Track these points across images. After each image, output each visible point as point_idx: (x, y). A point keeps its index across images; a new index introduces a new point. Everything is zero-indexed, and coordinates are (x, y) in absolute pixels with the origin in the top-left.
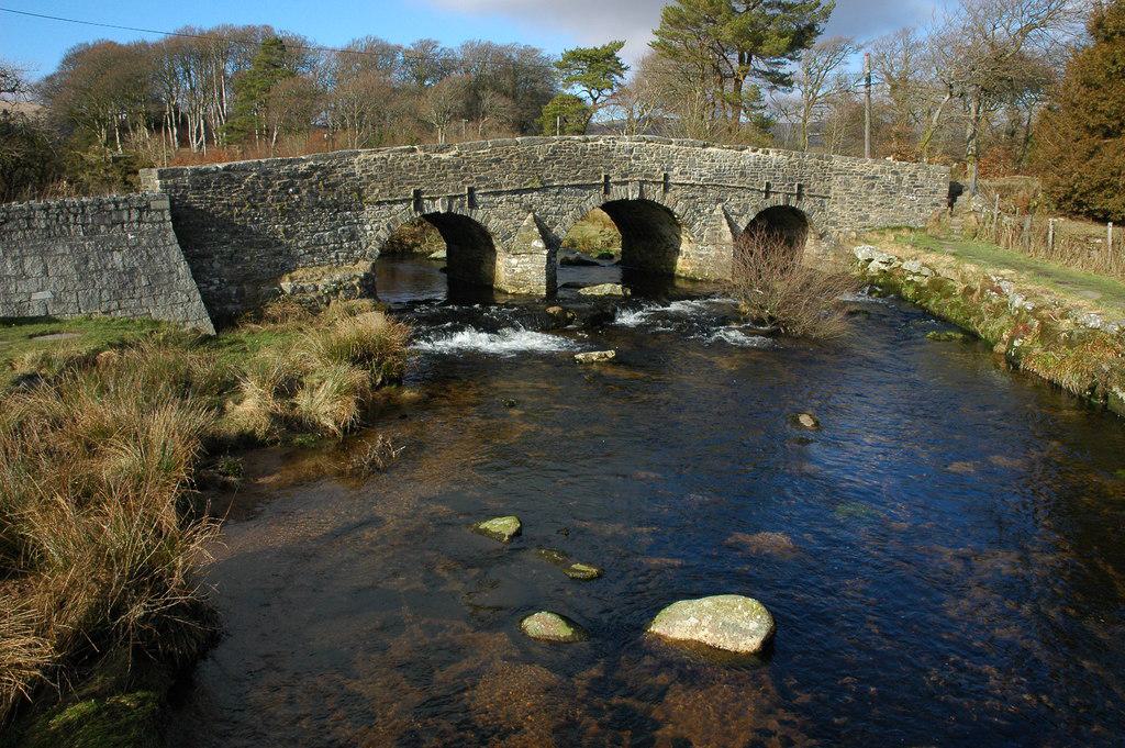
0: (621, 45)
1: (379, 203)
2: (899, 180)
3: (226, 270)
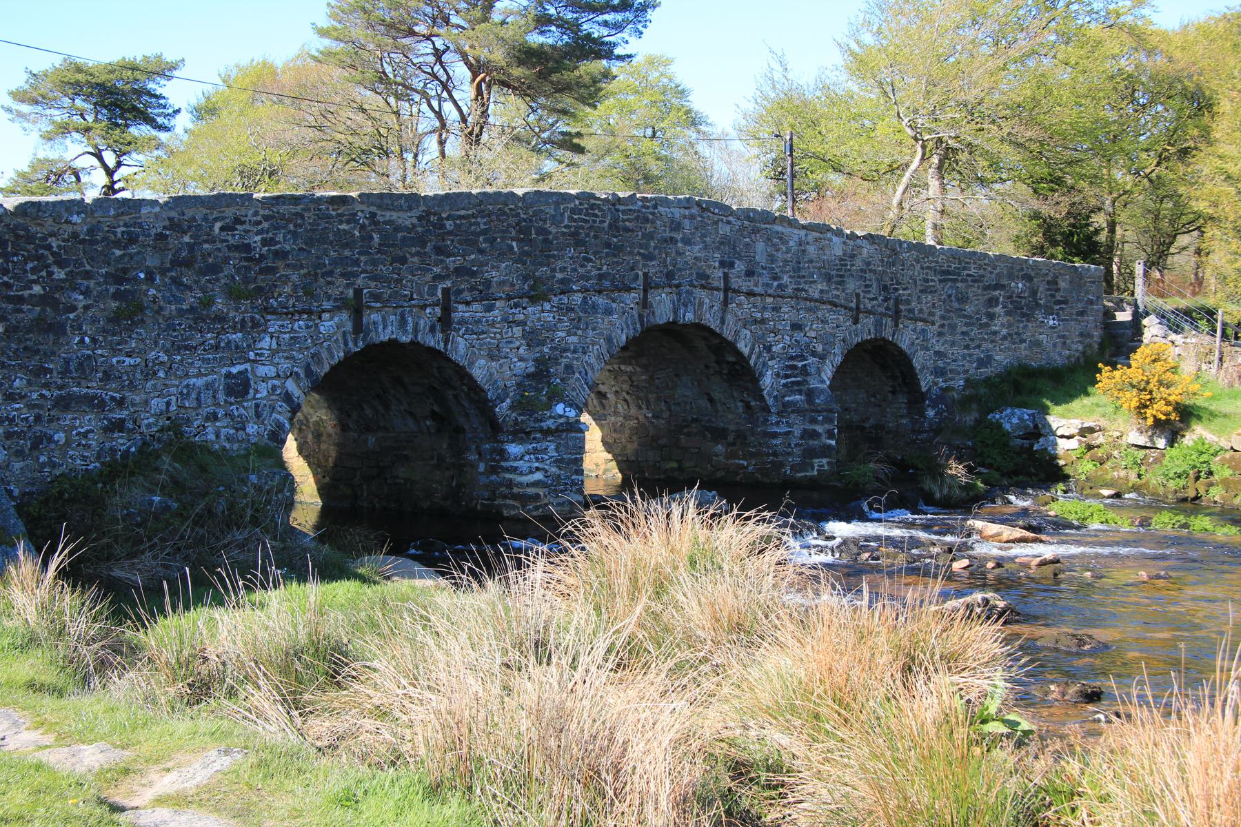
0: (164, 70)
1: (290, 314)
2: (1034, 293)
3: (18, 465)
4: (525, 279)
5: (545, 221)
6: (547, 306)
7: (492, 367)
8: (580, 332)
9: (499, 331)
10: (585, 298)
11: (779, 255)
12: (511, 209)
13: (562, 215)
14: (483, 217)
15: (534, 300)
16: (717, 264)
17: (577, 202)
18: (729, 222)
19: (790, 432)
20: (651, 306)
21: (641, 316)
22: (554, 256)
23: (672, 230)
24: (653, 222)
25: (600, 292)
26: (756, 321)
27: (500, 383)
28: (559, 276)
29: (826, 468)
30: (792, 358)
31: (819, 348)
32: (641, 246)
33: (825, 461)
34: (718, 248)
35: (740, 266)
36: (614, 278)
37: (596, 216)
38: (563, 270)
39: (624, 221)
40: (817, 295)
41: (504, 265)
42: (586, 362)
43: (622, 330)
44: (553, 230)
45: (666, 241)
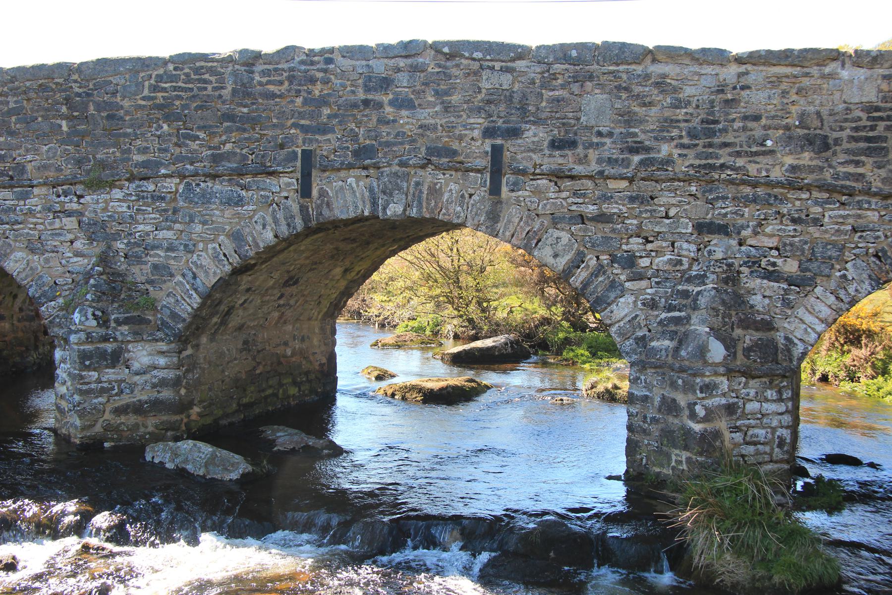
4: (79, 162)
5: (114, 94)
6: (117, 194)
7: (34, 261)
8: (178, 226)
9: (40, 221)
10: (188, 184)
11: (654, 111)
12: (57, 84)
13: (140, 85)
14: (15, 95)
15: (96, 185)
16: (476, 133)
17: (171, 67)
18: (508, 70)
19: (646, 397)
20: (322, 193)
21: (303, 209)
22: (126, 135)
23: (367, 89)
24: (326, 82)
25: (214, 177)
26: (582, 218)
27: (48, 279)
28: (138, 158)
29: (685, 467)
30: (689, 280)
31: (791, 267)
32: (301, 115)
33: (685, 455)
34: (479, 110)
35: (534, 134)
36: (245, 157)
37: (205, 81)
38: (144, 151)
39: (260, 84)
40: (777, 174)
41: (46, 148)
42: (194, 263)
43: (264, 227)
44: (126, 103)
45: (354, 106)
